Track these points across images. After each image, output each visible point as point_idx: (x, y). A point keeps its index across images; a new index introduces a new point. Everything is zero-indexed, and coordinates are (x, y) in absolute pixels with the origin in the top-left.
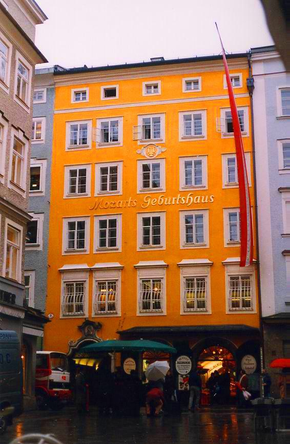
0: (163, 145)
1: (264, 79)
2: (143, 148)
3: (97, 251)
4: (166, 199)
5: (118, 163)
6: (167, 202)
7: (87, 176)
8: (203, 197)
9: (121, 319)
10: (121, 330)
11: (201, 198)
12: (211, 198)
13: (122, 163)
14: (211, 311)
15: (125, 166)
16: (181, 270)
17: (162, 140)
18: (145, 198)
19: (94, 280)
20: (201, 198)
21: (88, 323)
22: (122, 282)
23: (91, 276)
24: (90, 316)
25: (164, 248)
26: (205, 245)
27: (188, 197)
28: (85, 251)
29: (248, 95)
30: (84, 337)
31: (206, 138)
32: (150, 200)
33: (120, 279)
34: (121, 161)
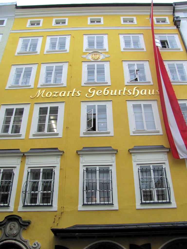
2: (87, 54)
3: (34, 135)
4: (112, 91)
5: (63, 64)
6: (113, 93)
7: (32, 73)
9: (55, 214)
10: (56, 227)
11: (147, 92)
13: (67, 64)
14: (175, 203)
17: (106, 50)
19: (26, 167)
20: (147, 92)
21: (12, 218)
24: (16, 209)
27: (134, 90)
28: (20, 136)
29: (175, 28)
30: (5, 238)
31: (145, 50)
34: (67, 62)
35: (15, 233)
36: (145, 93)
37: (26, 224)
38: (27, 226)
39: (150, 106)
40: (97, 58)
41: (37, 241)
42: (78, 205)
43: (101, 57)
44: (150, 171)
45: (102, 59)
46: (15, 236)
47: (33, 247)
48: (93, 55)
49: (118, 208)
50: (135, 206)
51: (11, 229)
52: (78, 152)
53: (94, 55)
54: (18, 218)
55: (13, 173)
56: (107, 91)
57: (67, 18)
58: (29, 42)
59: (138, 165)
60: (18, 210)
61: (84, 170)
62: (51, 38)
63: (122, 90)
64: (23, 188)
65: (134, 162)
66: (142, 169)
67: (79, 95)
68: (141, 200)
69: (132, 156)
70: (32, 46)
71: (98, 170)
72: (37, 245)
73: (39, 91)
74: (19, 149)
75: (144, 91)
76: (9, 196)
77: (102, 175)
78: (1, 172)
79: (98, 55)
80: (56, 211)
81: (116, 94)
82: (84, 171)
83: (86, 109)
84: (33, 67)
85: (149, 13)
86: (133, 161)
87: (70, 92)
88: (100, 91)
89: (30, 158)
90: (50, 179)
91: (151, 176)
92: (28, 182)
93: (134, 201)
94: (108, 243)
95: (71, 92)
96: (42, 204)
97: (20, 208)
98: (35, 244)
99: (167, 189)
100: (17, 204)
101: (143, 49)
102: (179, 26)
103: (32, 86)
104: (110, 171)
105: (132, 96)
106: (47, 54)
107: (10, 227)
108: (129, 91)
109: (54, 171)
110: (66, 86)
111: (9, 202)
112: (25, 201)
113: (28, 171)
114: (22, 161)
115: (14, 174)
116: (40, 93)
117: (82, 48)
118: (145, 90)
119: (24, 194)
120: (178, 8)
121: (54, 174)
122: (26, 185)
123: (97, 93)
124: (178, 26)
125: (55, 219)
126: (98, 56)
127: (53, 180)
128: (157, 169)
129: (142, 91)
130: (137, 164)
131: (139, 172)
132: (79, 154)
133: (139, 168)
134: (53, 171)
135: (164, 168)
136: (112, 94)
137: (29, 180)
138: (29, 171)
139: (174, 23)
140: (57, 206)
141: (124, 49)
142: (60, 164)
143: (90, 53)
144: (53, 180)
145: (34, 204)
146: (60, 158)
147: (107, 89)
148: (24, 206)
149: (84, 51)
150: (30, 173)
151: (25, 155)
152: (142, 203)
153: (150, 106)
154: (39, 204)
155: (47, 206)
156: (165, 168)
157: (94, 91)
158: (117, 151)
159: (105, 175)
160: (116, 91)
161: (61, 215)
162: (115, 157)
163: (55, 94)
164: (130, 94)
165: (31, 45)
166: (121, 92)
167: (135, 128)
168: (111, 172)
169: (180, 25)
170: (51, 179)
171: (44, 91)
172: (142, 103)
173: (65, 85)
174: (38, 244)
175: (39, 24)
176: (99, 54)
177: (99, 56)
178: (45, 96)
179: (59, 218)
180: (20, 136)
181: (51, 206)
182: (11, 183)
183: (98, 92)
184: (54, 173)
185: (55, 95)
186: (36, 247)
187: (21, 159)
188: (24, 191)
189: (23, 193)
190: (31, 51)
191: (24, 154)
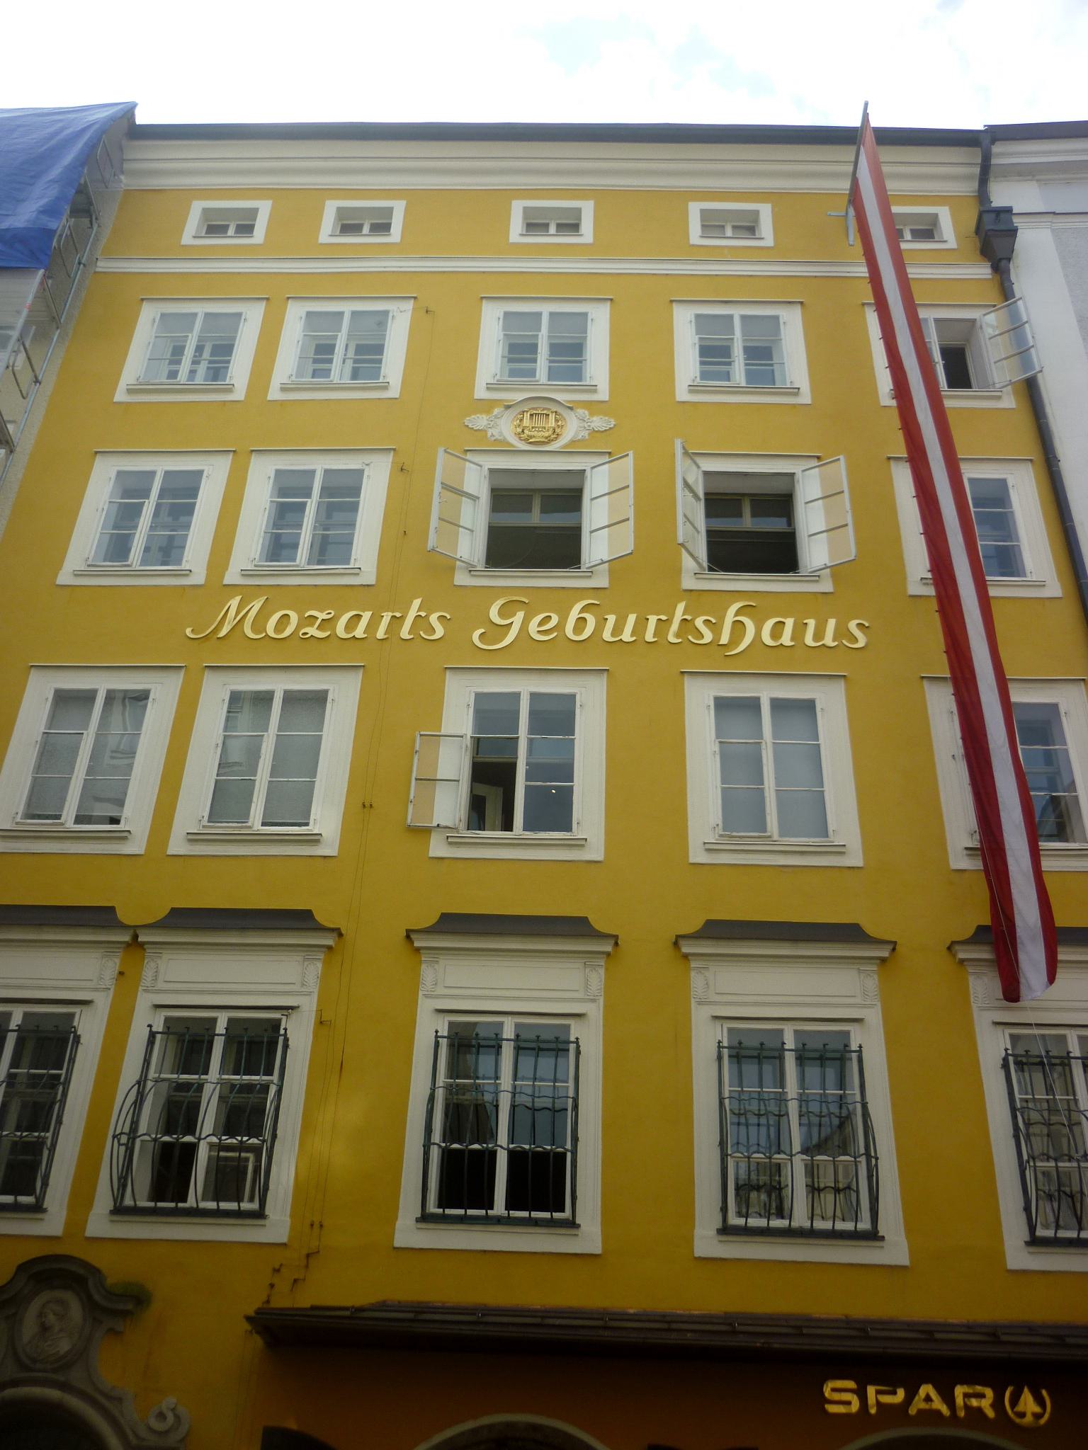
0: (594, 407)
1: (1053, 231)
2: (496, 411)
3: (193, 838)
4: (612, 619)
5: (367, 458)
6: (618, 629)
7: (199, 501)
8: (812, 623)
11: (800, 629)
12: (852, 625)
15: (401, 469)
16: (697, 981)
17: (595, 391)
18: (500, 602)
19: (144, 1001)
20: (800, 629)
22: (321, 1022)
23: (126, 981)
25: (595, 852)
26: (840, 851)
28: (123, 837)
29: (983, 271)
31: (806, 398)
32: (520, 615)
33: (309, 1005)
35: (62, 1352)
36: (786, 640)
37: (121, 1307)
38: (125, 1314)
39: (808, 707)
40: (546, 434)
41: (171, 1400)
42: (396, 1218)
43: (573, 428)
44: (781, 1058)
45: (573, 442)
46: (65, 1364)
47: (150, 1429)
48: (527, 416)
49: (600, 1245)
50: (689, 1241)
51: (45, 1329)
52: (413, 936)
53: (531, 415)
54: (81, 1271)
55: (75, 1032)
56: (584, 619)
57: (399, 198)
58: (191, 331)
59: (718, 1023)
60: (84, 1229)
61: (437, 1032)
62: (309, 314)
63: (664, 618)
64: (118, 1121)
65: (700, 1003)
66: (741, 1048)
67: (439, 632)
68: (724, 1209)
69: (693, 974)
70: (206, 354)
71: (507, 1040)
72: (171, 1418)
73: (234, 603)
74: (112, 910)
75: (784, 623)
76: (46, 1153)
77: (527, 1062)
78: (13, 1026)
79: (552, 417)
80: (285, 1244)
81: (632, 636)
82: (437, 1037)
83: (471, 710)
84: (207, 470)
85: (846, 185)
86: (693, 1001)
87: (393, 617)
88: (550, 617)
89: (167, 955)
90: (261, 1073)
91: (782, 1084)
92: (150, 1084)
93: (688, 1217)
94: (535, 1428)
95: (398, 615)
96: (211, 1205)
97: (99, 1223)
98: (161, 1416)
99: (863, 1159)
100: (81, 1199)
101: (796, 392)
102: (1003, 263)
103: (199, 578)
104: (572, 1047)
105: (716, 647)
106: (282, 403)
107: (41, 1315)
108: (699, 622)
109: (285, 1034)
110: (372, 581)
111: (45, 1184)
112: (123, 1186)
113: (150, 1026)
114: (121, 973)
115: (79, 1037)
116: (237, 613)
117: (472, 372)
118: (790, 622)
119: (123, 1149)
120: (1004, 154)
121: (286, 1046)
122: (135, 1102)
123: (533, 627)
124: (1000, 260)
125: (272, 1286)
126: (552, 422)
127: (275, 1081)
128: (816, 1050)
129: (769, 624)
130: (716, 1018)
131: (720, 1058)
132: (418, 950)
133: (719, 1042)
134: (282, 1032)
135: (854, 1047)
136: (613, 635)
137: (152, 1074)
138: (159, 1026)
139: (978, 245)
140: (288, 1219)
141: (693, 389)
142: (315, 997)
143: (508, 407)
144: (275, 1078)
145: (172, 1205)
146: (319, 965)
147: (583, 610)
148: (119, 1210)
149: (480, 393)
150: (159, 1037)
151: (139, 940)
152: (726, 1230)
153: (808, 707)
154: (195, 1206)
155: (239, 1214)
156: (860, 1047)
157: (519, 618)
158: (616, 944)
159: (546, 1063)
160: (632, 618)
161: (307, 1266)
162: (602, 971)
163: (312, 625)
164: (708, 637)
165: (199, 349)
166: (660, 622)
167: (720, 823)
168: (578, 1053)
169: (1009, 259)
170: (269, 1072)
171: (257, 605)
172: (766, 692)
173: (369, 577)
174: (177, 1417)
175: (246, 229)
176: (560, 410)
177: (557, 421)
178: (261, 633)
179: (295, 1281)
180: (123, 837)
181: (260, 1214)
182: (61, 1088)
183: (540, 624)
184: (286, 1040)
185: (312, 631)
186: (167, 1432)
187: (118, 961)
188: (121, 1133)
189: (120, 1144)
190: (199, 379)
191: (135, 931)
